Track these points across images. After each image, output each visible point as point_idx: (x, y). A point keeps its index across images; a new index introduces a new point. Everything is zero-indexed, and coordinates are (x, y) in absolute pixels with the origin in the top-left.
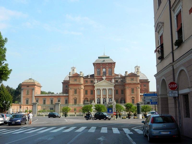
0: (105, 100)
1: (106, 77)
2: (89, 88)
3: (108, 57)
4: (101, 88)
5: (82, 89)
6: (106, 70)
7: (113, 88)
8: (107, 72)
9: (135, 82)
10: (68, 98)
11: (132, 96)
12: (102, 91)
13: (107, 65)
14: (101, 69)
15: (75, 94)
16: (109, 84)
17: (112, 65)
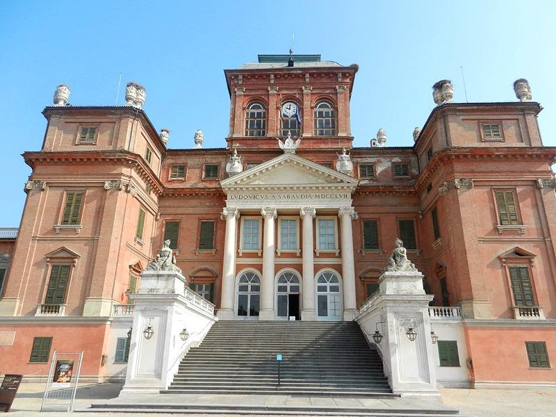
0: (289, 285)
1: (298, 141)
2: (190, 211)
3: (316, 58)
4: (270, 207)
5: (122, 194)
6: (301, 109)
7: (344, 205)
8: (309, 119)
9: (512, 142)
10: (10, 261)
11: (510, 247)
12: (270, 223)
13: (305, 84)
14: (273, 103)
15: (65, 222)
16: (320, 181)
17: (334, 81)
